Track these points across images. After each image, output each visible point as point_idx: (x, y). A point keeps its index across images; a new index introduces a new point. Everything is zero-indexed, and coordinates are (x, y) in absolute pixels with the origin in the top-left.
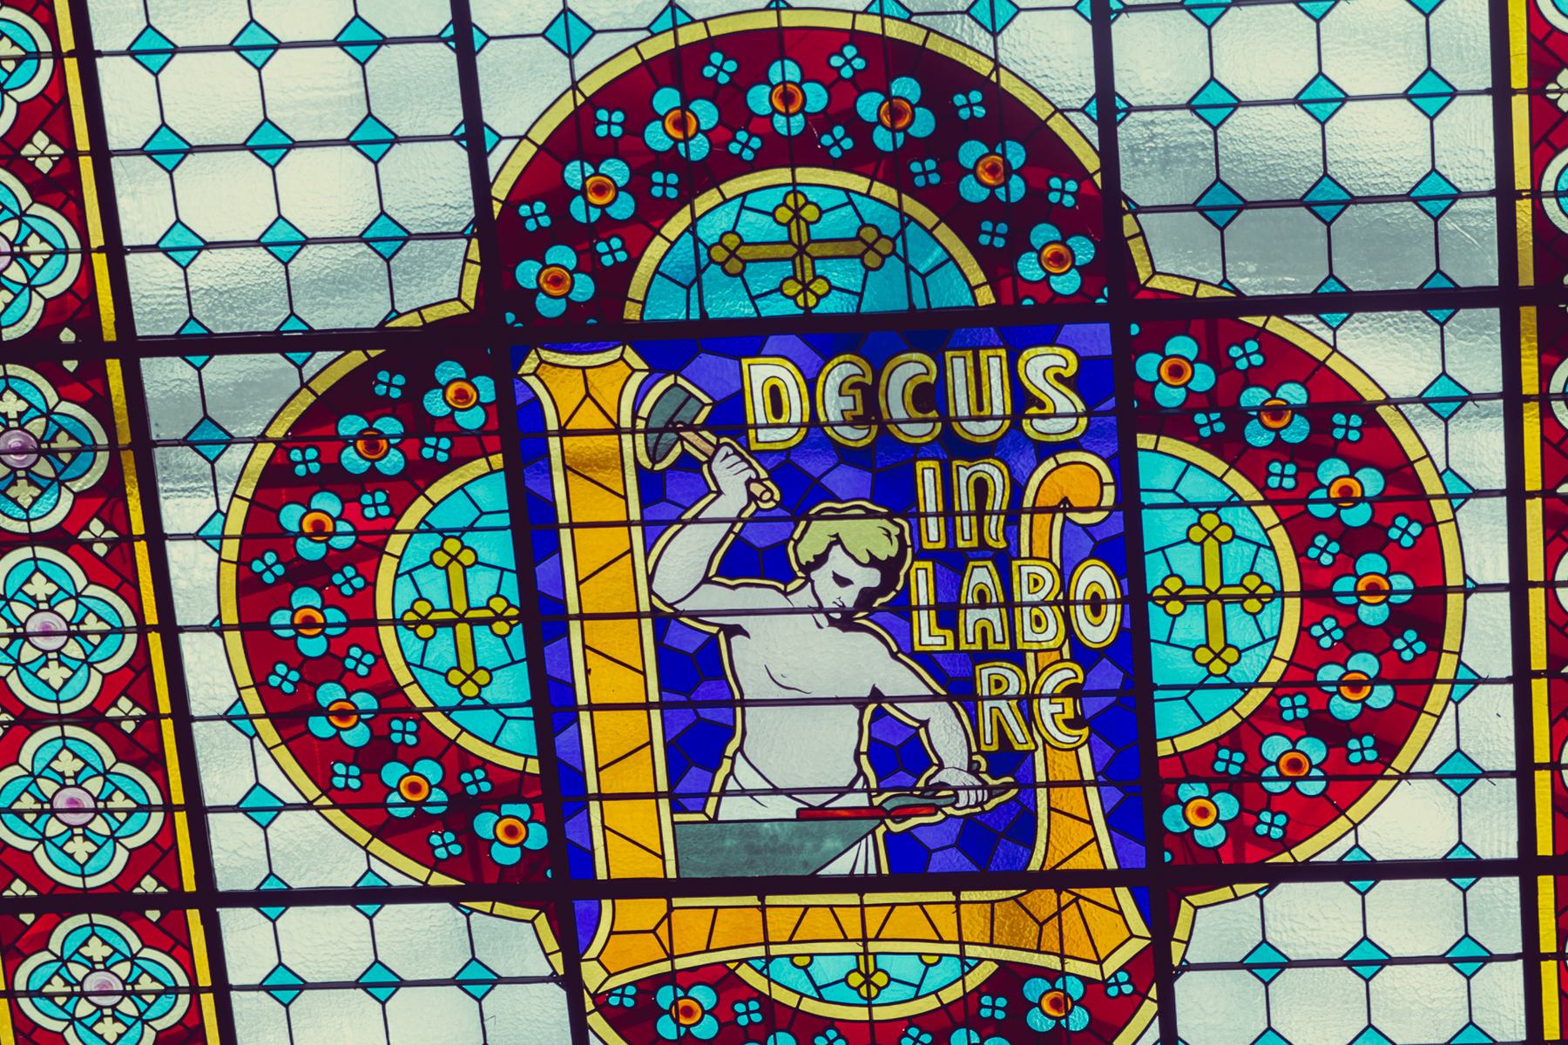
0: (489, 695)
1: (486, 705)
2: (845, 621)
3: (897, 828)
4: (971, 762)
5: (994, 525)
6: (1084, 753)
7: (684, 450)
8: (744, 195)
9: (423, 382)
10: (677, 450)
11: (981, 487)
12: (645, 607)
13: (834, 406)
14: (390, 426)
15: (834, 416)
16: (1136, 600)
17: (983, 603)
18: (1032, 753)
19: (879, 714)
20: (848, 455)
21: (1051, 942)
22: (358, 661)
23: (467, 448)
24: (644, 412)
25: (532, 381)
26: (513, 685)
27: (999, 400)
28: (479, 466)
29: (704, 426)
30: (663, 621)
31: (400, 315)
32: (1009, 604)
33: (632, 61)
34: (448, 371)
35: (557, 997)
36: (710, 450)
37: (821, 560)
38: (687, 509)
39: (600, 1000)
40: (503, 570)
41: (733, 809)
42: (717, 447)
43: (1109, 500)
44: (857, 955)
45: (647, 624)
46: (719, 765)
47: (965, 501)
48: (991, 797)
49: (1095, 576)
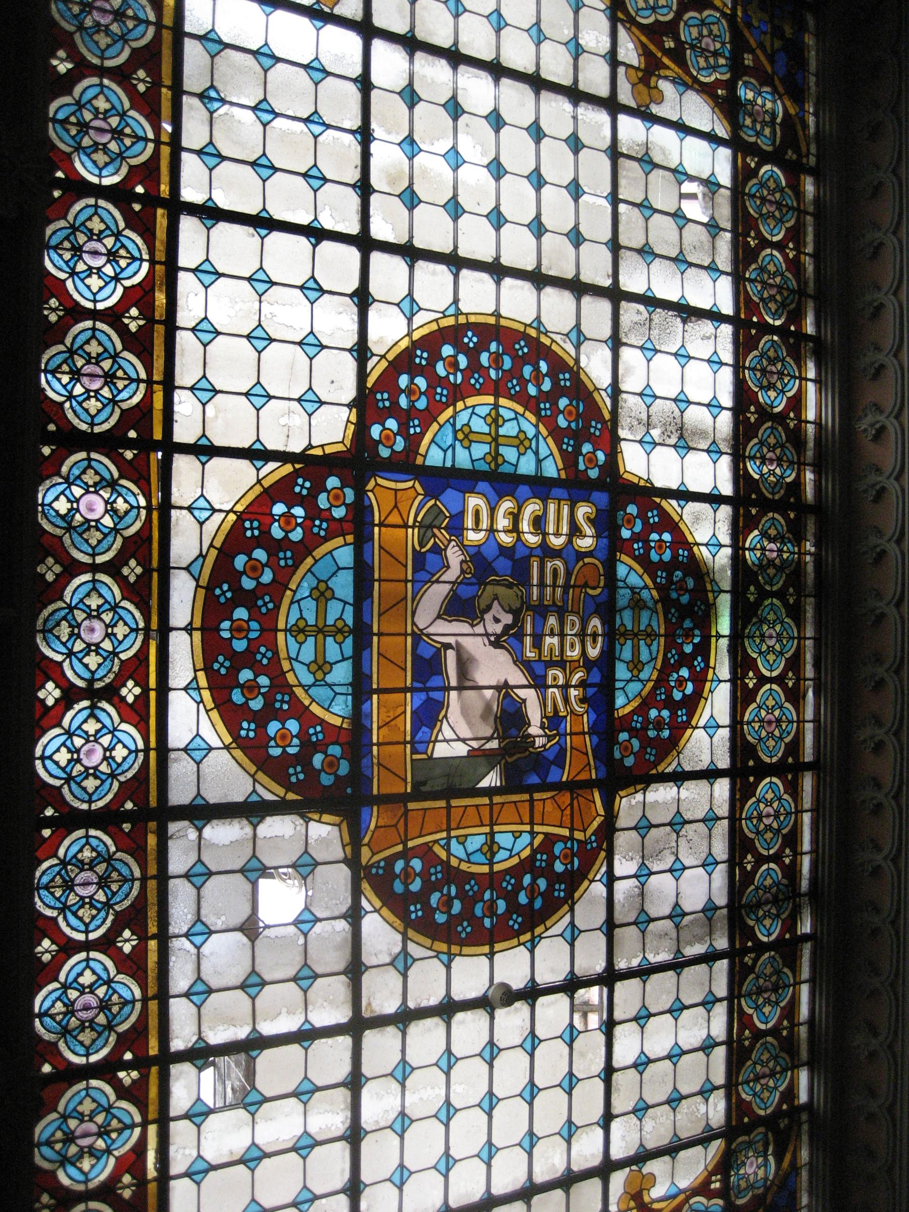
0: (329, 679)
1: (327, 684)
2: (496, 643)
3: (510, 760)
4: (542, 723)
5: (559, 591)
6: (585, 716)
7: (435, 542)
8: (474, 406)
9: (319, 487)
10: (432, 541)
11: (555, 572)
12: (409, 631)
13: (502, 523)
14: (299, 511)
15: (500, 528)
16: (612, 635)
17: (552, 634)
18: (565, 717)
19: (507, 695)
20: (504, 551)
21: (567, 820)
22: (263, 655)
23: (336, 529)
24: (419, 519)
25: (370, 494)
26: (342, 673)
27: (565, 529)
28: (339, 541)
29: (445, 528)
30: (418, 637)
31: (313, 447)
32: (562, 635)
33: (434, 327)
34: (333, 482)
35: (343, 873)
36: (446, 543)
37: (489, 608)
38: (434, 575)
39: (368, 868)
40: (345, 603)
41: (441, 751)
42: (450, 541)
43: (602, 584)
44: (486, 834)
45: (409, 639)
46: (435, 726)
47: (549, 581)
48: (549, 741)
49: (595, 623)
